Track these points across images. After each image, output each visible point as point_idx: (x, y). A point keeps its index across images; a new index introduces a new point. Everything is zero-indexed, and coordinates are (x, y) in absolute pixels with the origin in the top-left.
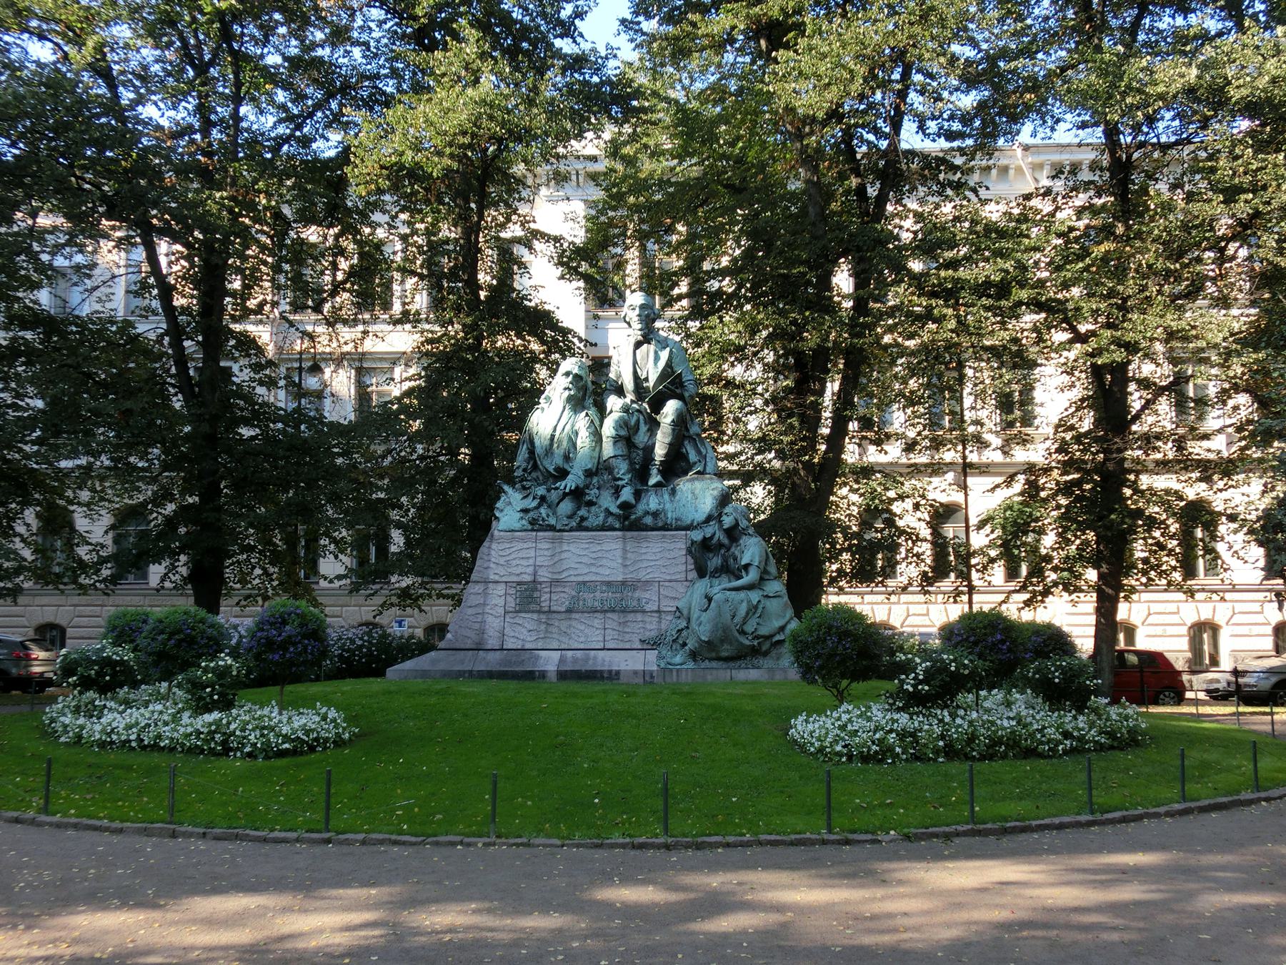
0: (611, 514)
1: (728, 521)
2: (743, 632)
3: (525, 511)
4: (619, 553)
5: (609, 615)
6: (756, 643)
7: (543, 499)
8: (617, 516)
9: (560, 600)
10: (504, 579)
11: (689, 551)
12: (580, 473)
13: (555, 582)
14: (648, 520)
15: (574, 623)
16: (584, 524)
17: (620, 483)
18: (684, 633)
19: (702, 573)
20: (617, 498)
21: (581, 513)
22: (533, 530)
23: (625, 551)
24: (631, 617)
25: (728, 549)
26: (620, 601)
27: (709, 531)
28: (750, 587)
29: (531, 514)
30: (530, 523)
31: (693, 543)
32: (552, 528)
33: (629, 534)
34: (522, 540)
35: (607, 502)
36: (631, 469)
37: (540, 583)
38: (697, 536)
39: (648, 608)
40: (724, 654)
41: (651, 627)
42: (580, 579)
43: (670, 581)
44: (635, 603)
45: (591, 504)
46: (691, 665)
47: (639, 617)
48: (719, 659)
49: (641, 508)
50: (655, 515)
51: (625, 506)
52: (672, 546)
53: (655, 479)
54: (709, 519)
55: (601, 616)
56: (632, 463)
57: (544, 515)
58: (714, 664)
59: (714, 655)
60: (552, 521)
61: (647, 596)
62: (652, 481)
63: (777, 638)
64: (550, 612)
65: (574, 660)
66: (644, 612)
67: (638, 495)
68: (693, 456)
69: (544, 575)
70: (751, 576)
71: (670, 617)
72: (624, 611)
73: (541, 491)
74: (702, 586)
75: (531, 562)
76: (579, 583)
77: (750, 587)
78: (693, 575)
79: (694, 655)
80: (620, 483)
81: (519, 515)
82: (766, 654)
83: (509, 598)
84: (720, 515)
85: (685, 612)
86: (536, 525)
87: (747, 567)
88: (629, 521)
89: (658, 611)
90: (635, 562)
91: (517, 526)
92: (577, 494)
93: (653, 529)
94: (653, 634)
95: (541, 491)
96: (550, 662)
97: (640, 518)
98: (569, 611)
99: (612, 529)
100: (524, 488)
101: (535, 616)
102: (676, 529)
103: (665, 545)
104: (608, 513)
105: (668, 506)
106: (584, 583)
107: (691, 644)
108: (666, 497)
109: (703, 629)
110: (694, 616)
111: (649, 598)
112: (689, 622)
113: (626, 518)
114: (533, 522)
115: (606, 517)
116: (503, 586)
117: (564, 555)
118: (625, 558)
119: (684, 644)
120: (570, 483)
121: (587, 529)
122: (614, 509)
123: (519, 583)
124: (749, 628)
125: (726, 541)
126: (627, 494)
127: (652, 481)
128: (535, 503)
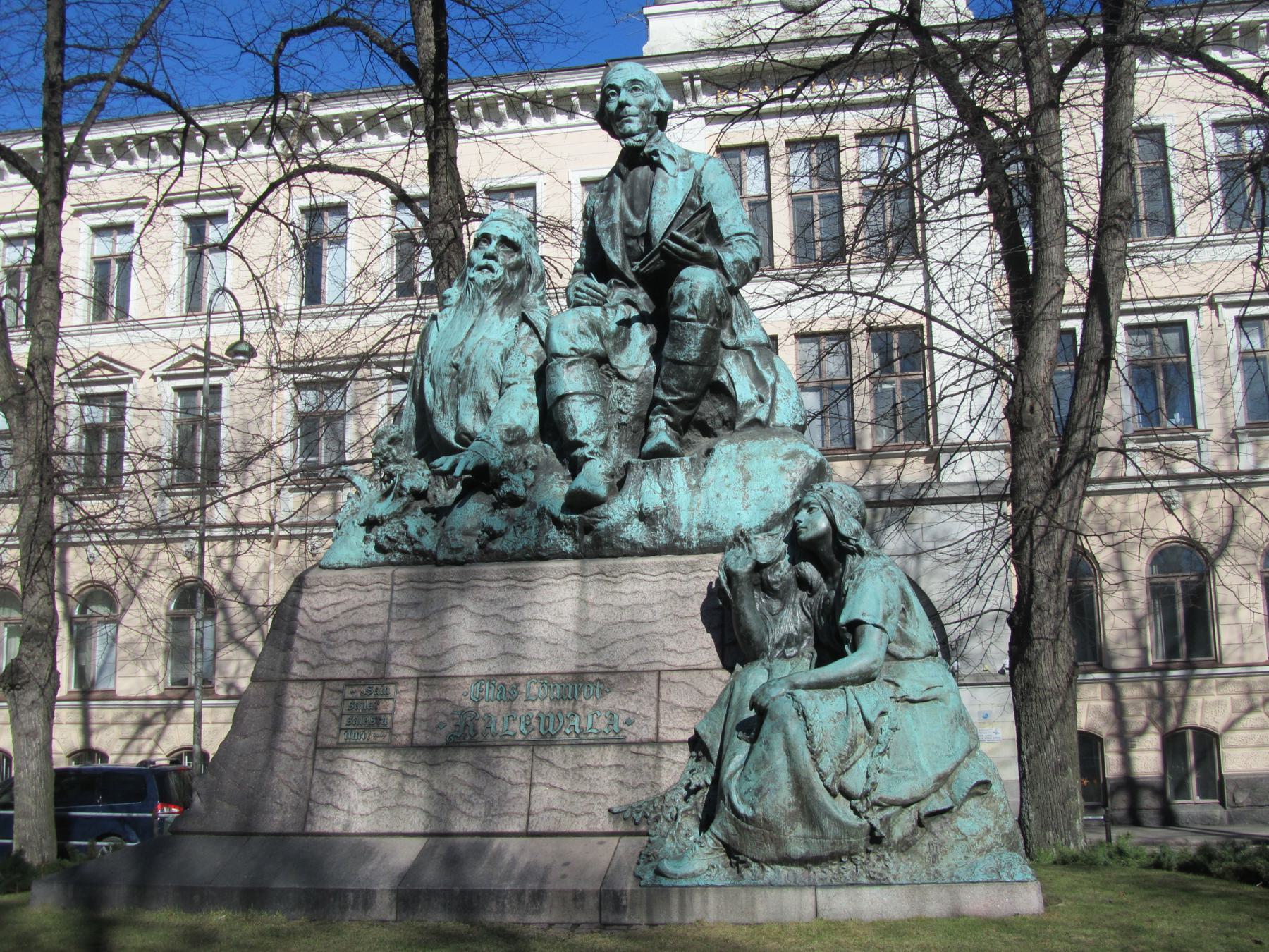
6: (875, 818)
14: (636, 531)
22: (388, 564)
30: (379, 548)
33: (593, 565)
37: (395, 681)
40: (798, 849)
43: (684, 670)
57: (412, 530)
59: (770, 851)
61: (632, 706)
63: (935, 804)
68: (744, 390)
75: (379, 633)
82: (906, 845)
93: (648, 552)
123: (351, 682)
124: (855, 782)
128: (398, 505)
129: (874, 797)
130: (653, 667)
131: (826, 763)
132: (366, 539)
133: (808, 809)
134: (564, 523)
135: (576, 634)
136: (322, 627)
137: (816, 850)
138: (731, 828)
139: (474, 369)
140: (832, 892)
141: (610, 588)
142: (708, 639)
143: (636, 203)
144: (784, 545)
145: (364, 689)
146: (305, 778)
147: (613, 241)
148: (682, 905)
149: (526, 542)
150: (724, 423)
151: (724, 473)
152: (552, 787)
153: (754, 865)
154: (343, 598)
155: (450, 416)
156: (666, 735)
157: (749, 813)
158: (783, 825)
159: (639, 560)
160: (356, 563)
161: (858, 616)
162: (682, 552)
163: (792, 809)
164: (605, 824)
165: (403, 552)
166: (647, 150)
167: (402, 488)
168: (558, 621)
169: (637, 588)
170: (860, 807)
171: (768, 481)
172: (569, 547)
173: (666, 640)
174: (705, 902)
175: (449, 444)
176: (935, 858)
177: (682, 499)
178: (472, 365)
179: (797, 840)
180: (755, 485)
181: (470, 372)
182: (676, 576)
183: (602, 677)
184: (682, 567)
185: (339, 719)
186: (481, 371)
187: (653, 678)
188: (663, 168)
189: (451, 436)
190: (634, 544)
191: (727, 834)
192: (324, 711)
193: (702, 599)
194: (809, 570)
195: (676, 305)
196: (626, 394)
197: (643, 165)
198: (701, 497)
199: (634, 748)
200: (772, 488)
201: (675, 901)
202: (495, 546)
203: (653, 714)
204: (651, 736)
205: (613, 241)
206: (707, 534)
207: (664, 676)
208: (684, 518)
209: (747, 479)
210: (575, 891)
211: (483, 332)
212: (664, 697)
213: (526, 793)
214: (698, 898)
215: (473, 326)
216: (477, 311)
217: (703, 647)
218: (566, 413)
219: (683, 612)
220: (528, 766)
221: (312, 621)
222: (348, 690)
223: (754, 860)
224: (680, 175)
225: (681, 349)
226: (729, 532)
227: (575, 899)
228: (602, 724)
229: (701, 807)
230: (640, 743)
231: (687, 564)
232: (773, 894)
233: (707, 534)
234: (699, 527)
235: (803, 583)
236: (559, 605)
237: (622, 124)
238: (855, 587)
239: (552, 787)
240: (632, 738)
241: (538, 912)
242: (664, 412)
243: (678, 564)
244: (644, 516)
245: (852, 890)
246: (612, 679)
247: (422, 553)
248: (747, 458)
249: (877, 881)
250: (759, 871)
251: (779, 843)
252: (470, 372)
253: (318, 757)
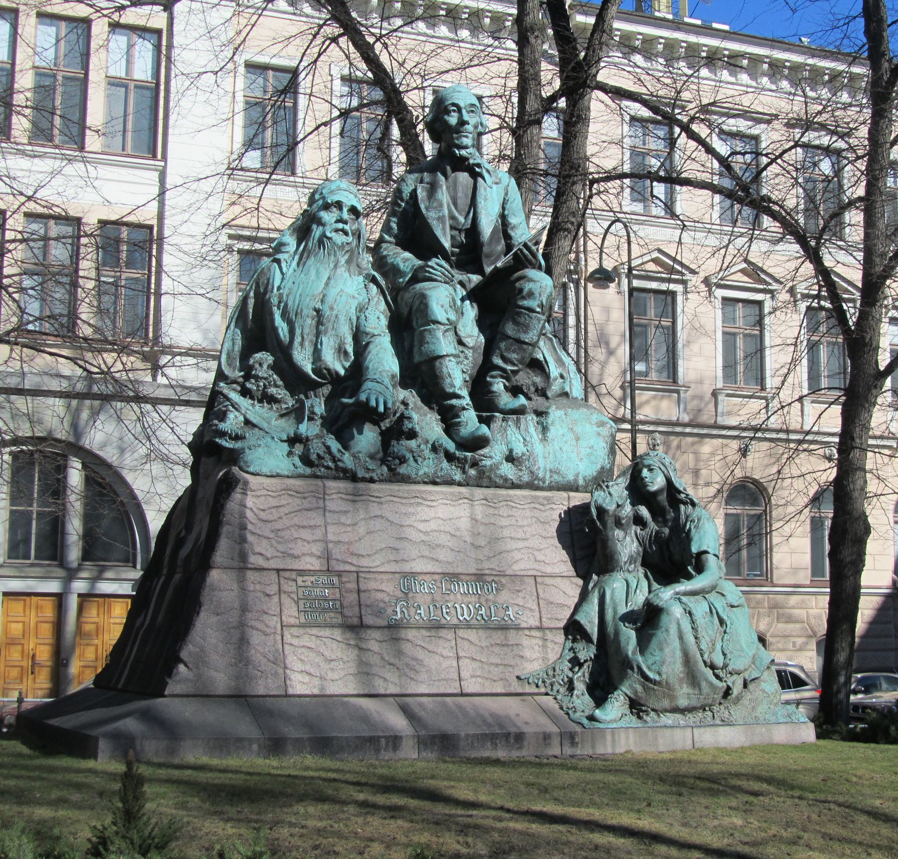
5: (461, 633)
10: (273, 564)
14: (507, 470)
22: (315, 476)
33: (479, 492)
40: (683, 702)
55: (450, 635)
59: (666, 703)
71: (560, 638)
75: (319, 534)
93: (514, 486)
99: (450, 482)
102: (550, 488)
103: (537, 514)
116: (274, 576)
129: (730, 668)
130: (530, 573)
132: (290, 454)
133: (692, 678)
134: (458, 459)
135: (472, 544)
136: (269, 525)
137: (694, 703)
138: (639, 688)
139: (337, 316)
140: (702, 730)
141: (491, 511)
142: (563, 555)
143: (459, 201)
144: (626, 492)
145: (313, 579)
146: (277, 650)
147: (444, 229)
148: (613, 741)
149: (426, 470)
150: (537, 390)
151: (561, 432)
152: (473, 659)
153: (652, 714)
154: (283, 502)
155: (309, 349)
156: (546, 623)
157: (657, 678)
158: (677, 687)
159: (511, 492)
160: (286, 473)
161: (704, 548)
162: (537, 488)
163: (682, 675)
165: (328, 468)
166: (471, 161)
167: (313, 413)
168: (458, 534)
169: (510, 513)
170: (721, 675)
171: (592, 442)
172: (458, 476)
173: (536, 553)
174: (627, 738)
175: (305, 375)
176: (754, 708)
177: (538, 448)
178: (335, 313)
179: (684, 695)
180: (583, 443)
181: (333, 318)
182: (537, 506)
183: (496, 579)
184: (542, 500)
185: (297, 603)
186: (342, 318)
187: (532, 581)
188: (483, 178)
189: (308, 368)
190: (506, 480)
191: (636, 692)
192: (283, 596)
193: (556, 524)
194: (644, 511)
195: (524, 298)
196: (466, 358)
197: (464, 171)
198: (549, 448)
199: (527, 632)
200: (595, 447)
201: (609, 737)
203: (535, 607)
204: (537, 624)
205: (444, 229)
206: (556, 477)
207: (539, 580)
208: (541, 463)
209: (577, 439)
210: (544, 733)
211: (341, 286)
212: (541, 595)
213: (455, 663)
214: (623, 735)
215: (329, 278)
216: (332, 266)
217: (558, 560)
218: (445, 370)
219: (544, 534)
220: (453, 643)
221: (260, 520)
222: (300, 579)
223: (653, 710)
224: (494, 186)
225: (526, 332)
226: (571, 477)
227: (545, 739)
229: (587, 675)
230: (530, 629)
231: (545, 498)
232: (668, 732)
233: (556, 477)
234: (551, 471)
235: (638, 520)
236: (435, 519)
237: (461, 137)
238: (696, 527)
239: (473, 659)
240: (524, 625)
241: (520, 748)
242: (502, 377)
243: (538, 497)
244: (510, 458)
245: (713, 729)
246: (503, 580)
247: (345, 470)
248: (575, 422)
249: (725, 723)
250: (656, 717)
251: (673, 698)
252: (333, 318)
253: (286, 633)
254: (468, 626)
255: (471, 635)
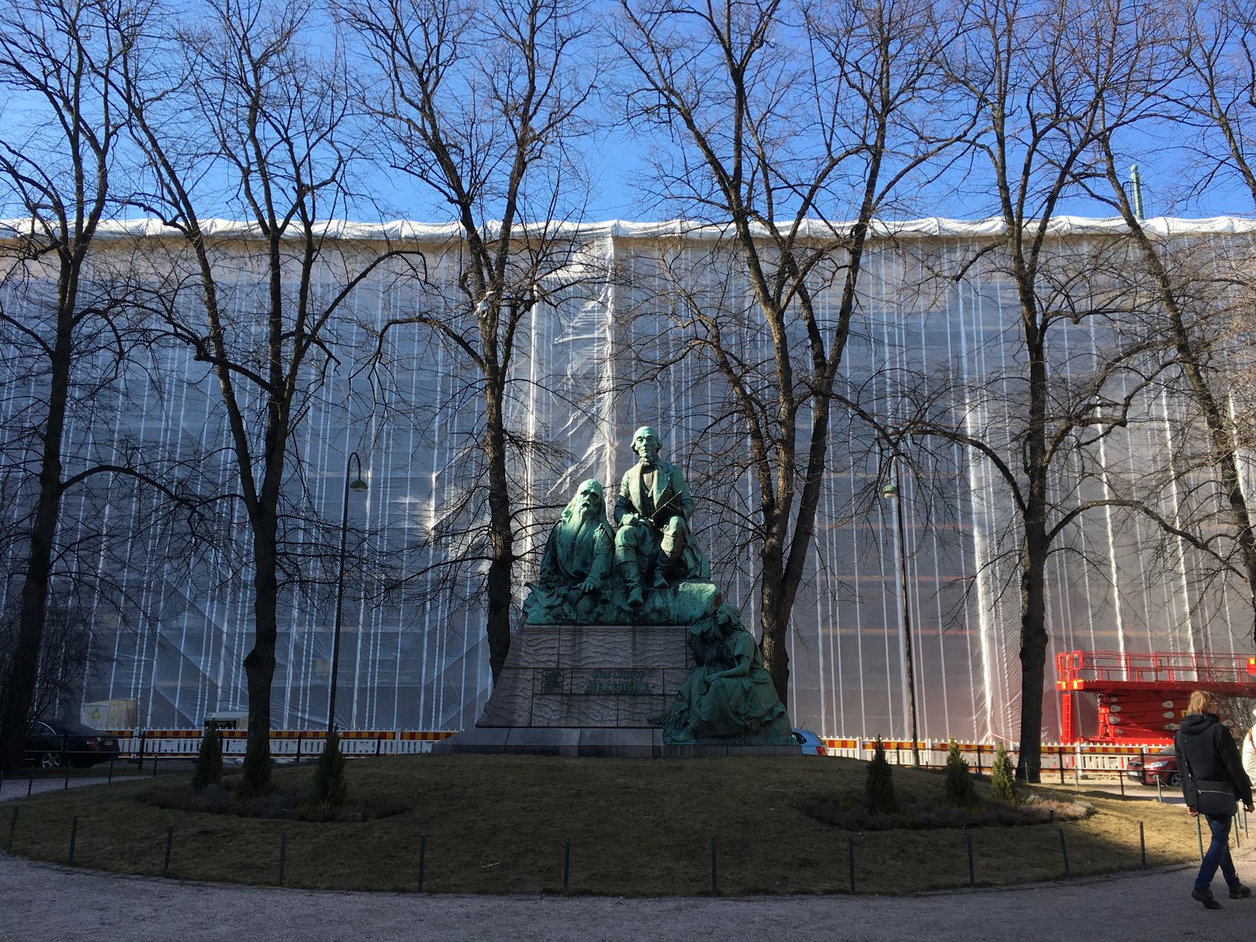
0: (623, 610)
1: (722, 618)
2: (737, 714)
3: (550, 607)
4: (629, 644)
7: (565, 597)
8: (628, 613)
9: (580, 685)
11: (689, 643)
12: (597, 576)
13: (575, 669)
14: (654, 616)
15: (592, 704)
16: (601, 619)
17: (630, 585)
18: (686, 714)
19: (700, 663)
20: (628, 597)
21: (597, 610)
23: (634, 642)
24: (640, 699)
25: (723, 642)
26: (629, 685)
27: (705, 626)
28: (741, 675)
29: (555, 611)
31: (693, 636)
32: (574, 623)
33: (638, 628)
34: (547, 632)
35: (619, 600)
36: (641, 574)
37: (563, 669)
38: (696, 630)
39: (655, 691)
40: (721, 733)
41: (658, 708)
42: (597, 666)
44: (643, 688)
45: (606, 602)
46: (693, 742)
47: (647, 699)
48: (718, 737)
49: (648, 608)
50: (660, 612)
51: (635, 604)
52: (674, 638)
53: (660, 581)
54: (705, 616)
56: (640, 568)
58: (712, 741)
60: (573, 616)
62: (657, 584)
63: (767, 719)
64: (571, 694)
65: (590, 738)
66: (651, 695)
67: (645, 595)
68: (691, 564)
69: (567, 663)
70: (744, 666)
72: (635, 694)
73: (563, 590)
74: (700, 673)
75: (555, 651)
76: (595, 670)
77: (741, 675)
78: (692, 664)
79: (695, 733)
80: (630, 585)
81: (544, 611)
82: (757, 733)
83: (537, 683)
84: (715, 612)
85: (686, 696)
86: (559, 620)
87: (739, 657)
88: (638, 619)
89: (663, 695)
90: (643, 652)
91: (544, 620)
92: (594, 594)
94: (659, 714)
95: (563, 590)
96: (572, 738)
97: (648, 615)
98: (587, 694)
100: (549, 588)
101: (559, 698)
104: (620, 610)
105: (670, 604)
106: (600, 670)
107: (692, 723)
108: (669, 596)
109: (703, 709)
110: (695, 699)
111: (655, 681)
112: (690, 702)
113: (636, 614)
114: (556, 617)
115: (619, 613)
117: (584, 646)
118: (634, 649)
119: (686, 724)
120: (588, 584)
121: (602, 624)
122: (627, 608)
124: (741, 710)
125: (719, 635)
126: (636, 594)
127: (657, 584)
131: (732, 703)
164: (645, 724)
202: (601, 619)
228: (643, 688)
254: (624, 693)
255: (627, 699)
